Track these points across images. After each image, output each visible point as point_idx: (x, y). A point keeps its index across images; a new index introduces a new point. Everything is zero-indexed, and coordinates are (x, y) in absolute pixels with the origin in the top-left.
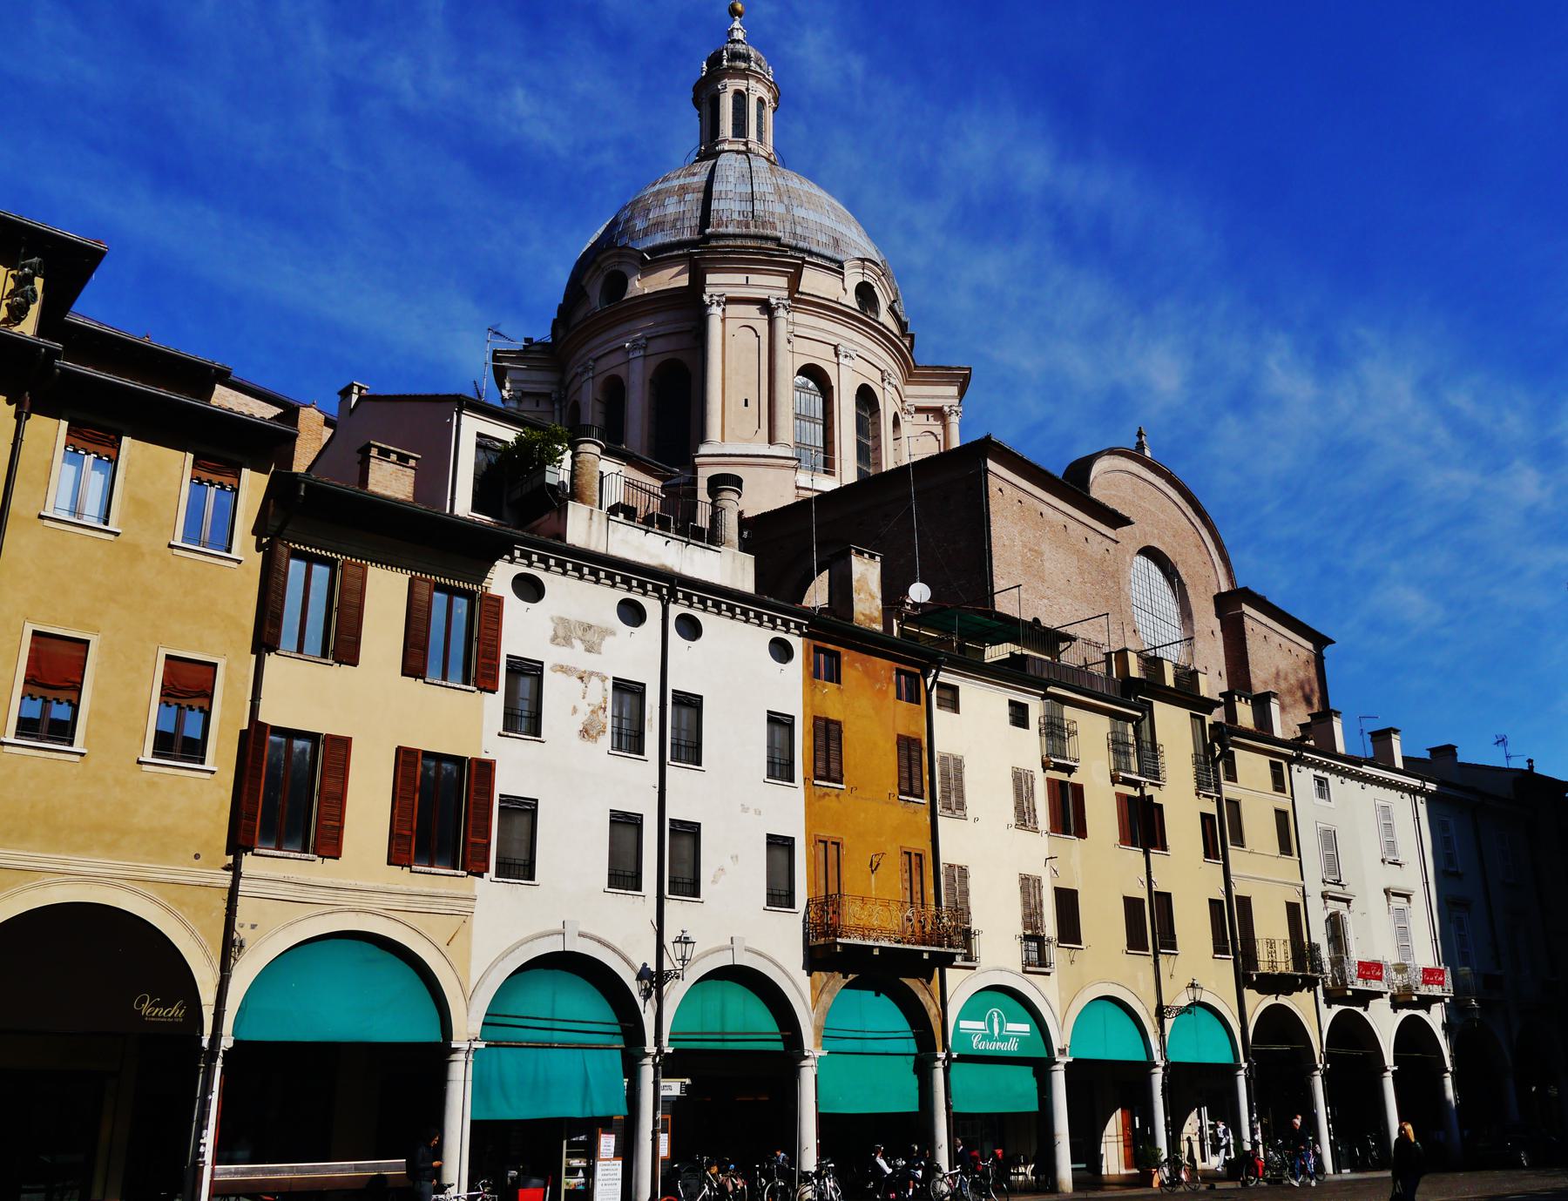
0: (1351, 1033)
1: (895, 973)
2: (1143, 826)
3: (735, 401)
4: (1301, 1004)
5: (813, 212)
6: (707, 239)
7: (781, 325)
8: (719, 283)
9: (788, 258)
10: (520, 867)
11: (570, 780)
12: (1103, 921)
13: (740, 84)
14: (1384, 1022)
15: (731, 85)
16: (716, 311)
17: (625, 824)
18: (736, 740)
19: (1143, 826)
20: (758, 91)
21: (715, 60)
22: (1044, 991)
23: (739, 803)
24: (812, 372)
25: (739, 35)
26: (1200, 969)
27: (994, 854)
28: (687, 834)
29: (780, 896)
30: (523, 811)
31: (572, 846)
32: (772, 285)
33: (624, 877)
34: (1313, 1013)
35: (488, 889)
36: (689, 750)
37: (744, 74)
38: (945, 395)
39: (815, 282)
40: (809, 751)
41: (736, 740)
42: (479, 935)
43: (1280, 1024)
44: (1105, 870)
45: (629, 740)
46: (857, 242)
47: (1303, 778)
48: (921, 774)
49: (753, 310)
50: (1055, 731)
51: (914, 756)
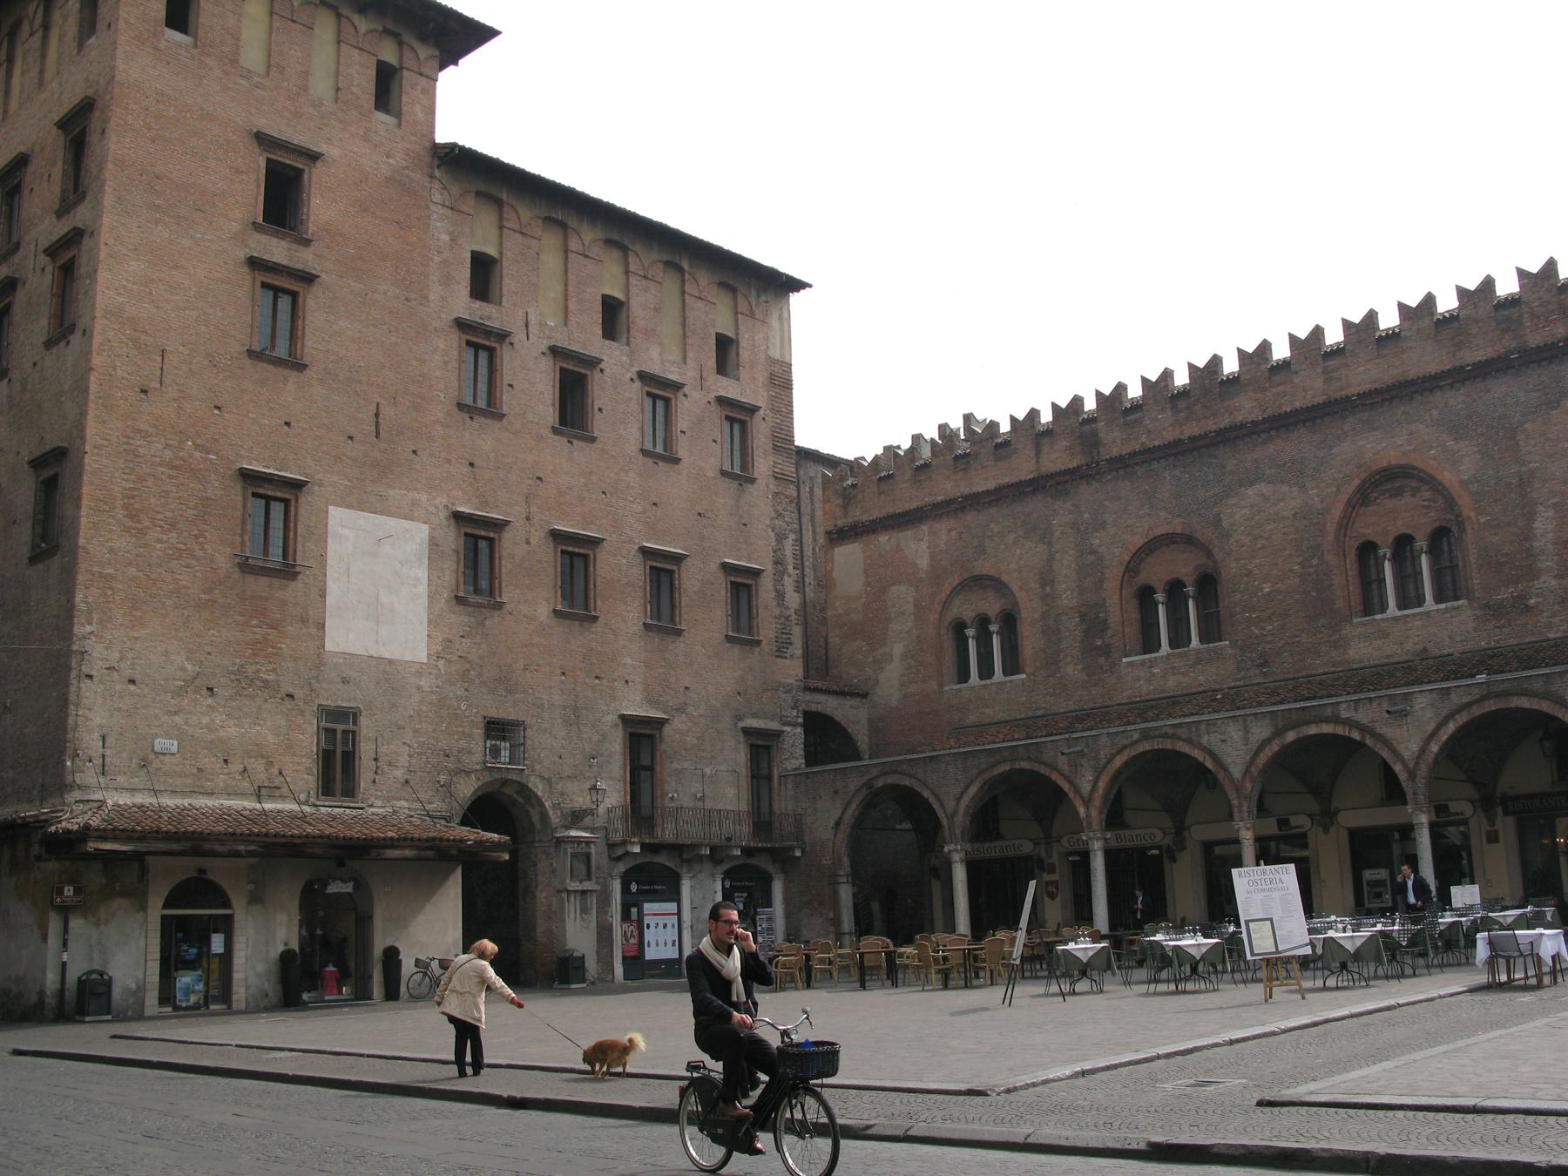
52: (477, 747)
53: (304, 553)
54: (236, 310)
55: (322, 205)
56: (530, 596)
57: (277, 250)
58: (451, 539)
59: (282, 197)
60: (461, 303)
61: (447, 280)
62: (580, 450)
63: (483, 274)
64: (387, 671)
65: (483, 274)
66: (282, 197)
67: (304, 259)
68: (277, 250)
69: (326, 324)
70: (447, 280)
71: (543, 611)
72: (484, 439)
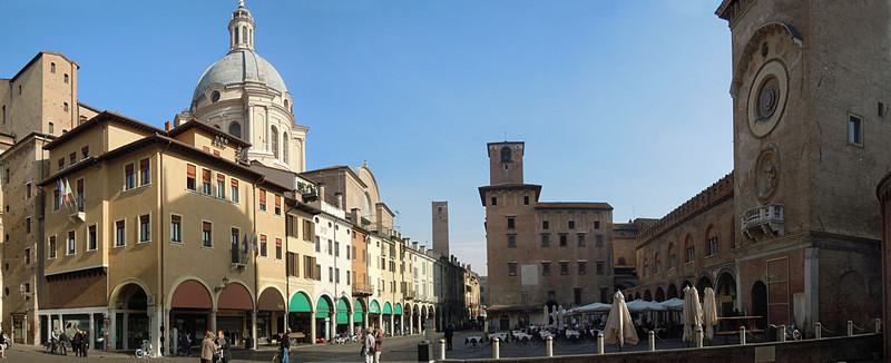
0: (416, 308)
1: (361, 297)
2: (392, 268)
3: (257, 138)
4: (410, 302)
5: (274, 78)
6: (245, 83)
7: (270, 115)
8: (252, 100)
9: (268, 92)
10: (319, 279)
11: (324, 260)
12: (388, 287)
13: (244, 24)
14: (420, 305)
15: (242, 24)
16: (251, 108)
17: (331, 268)
18: (343, 251)
19: (392, 268)
20: (250, 27)
21: (237, 14)
22: (380, 300)
23: (345, 265)
24: (274, 128)
25: (242, 4)
26: (399, 296)
27: (375, 273)
28: (337, 270)
29: (349, 283)
30: (319, 266)
31: (325, 274)
32: (266, 101)
33: (331, 280)
34: (412, 306)
35: (315, 282)
36: (337, 254)
37: (246, 20)
38: (302, 134)
39: (277, 100)
40: (352, 253)
41: (343, 251)
42: (317, 289)
43: (407, 307)
44: (388, 276)
45: (330, 253)
46: (283, 89)
47: (414, 256)
48: (366, 258)
49: (262, 109)
50: (383, 248)
51: (365, 252)
52: (546, 295)
53: (518, 273)
54: (505, 241)
55: (516, 223)
56: (556, 272)
57: (511, 232)
58: (541, 266)
59: (511, 223)
60: (542, 230)
61: (539, 228)
62: (564, 248)
63: (546, 225)
64: (532, 286)
65: (546, 225)
66: (511, 223)
67: (516, 231)
68: (511, 232)
69: (518, 240)
70: (539, 228)
71: (559, 275)
72: (546, 249)
